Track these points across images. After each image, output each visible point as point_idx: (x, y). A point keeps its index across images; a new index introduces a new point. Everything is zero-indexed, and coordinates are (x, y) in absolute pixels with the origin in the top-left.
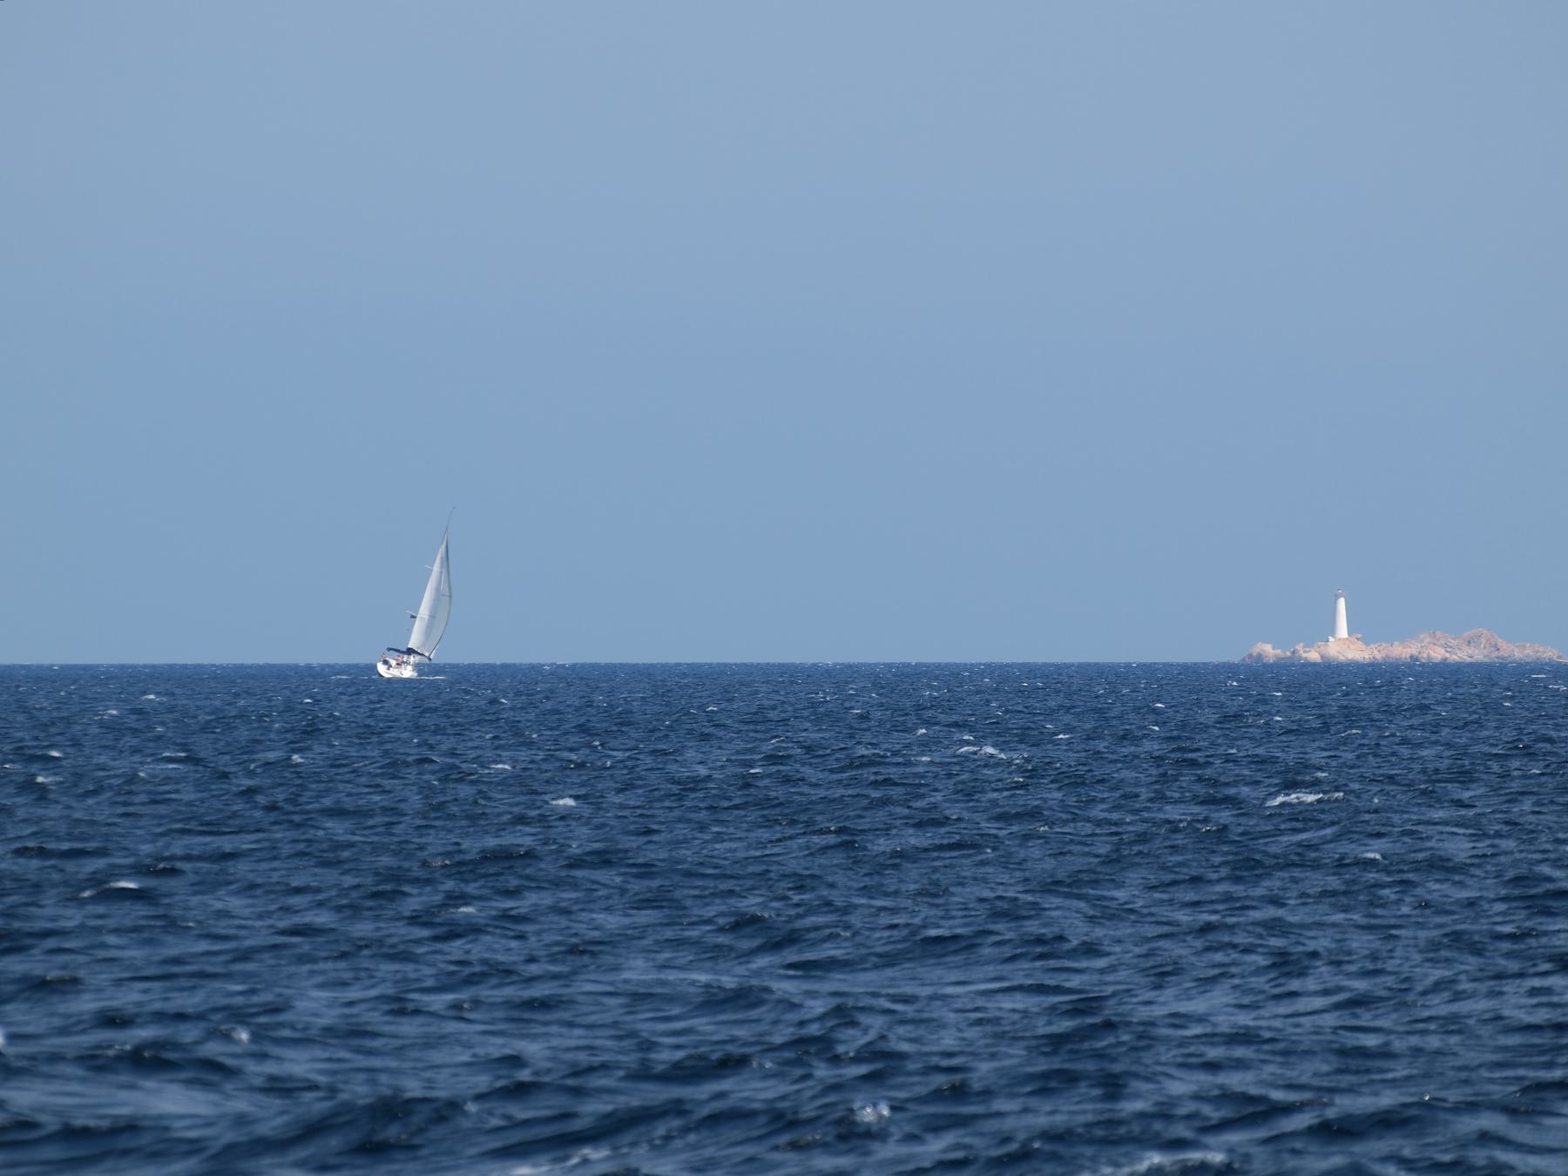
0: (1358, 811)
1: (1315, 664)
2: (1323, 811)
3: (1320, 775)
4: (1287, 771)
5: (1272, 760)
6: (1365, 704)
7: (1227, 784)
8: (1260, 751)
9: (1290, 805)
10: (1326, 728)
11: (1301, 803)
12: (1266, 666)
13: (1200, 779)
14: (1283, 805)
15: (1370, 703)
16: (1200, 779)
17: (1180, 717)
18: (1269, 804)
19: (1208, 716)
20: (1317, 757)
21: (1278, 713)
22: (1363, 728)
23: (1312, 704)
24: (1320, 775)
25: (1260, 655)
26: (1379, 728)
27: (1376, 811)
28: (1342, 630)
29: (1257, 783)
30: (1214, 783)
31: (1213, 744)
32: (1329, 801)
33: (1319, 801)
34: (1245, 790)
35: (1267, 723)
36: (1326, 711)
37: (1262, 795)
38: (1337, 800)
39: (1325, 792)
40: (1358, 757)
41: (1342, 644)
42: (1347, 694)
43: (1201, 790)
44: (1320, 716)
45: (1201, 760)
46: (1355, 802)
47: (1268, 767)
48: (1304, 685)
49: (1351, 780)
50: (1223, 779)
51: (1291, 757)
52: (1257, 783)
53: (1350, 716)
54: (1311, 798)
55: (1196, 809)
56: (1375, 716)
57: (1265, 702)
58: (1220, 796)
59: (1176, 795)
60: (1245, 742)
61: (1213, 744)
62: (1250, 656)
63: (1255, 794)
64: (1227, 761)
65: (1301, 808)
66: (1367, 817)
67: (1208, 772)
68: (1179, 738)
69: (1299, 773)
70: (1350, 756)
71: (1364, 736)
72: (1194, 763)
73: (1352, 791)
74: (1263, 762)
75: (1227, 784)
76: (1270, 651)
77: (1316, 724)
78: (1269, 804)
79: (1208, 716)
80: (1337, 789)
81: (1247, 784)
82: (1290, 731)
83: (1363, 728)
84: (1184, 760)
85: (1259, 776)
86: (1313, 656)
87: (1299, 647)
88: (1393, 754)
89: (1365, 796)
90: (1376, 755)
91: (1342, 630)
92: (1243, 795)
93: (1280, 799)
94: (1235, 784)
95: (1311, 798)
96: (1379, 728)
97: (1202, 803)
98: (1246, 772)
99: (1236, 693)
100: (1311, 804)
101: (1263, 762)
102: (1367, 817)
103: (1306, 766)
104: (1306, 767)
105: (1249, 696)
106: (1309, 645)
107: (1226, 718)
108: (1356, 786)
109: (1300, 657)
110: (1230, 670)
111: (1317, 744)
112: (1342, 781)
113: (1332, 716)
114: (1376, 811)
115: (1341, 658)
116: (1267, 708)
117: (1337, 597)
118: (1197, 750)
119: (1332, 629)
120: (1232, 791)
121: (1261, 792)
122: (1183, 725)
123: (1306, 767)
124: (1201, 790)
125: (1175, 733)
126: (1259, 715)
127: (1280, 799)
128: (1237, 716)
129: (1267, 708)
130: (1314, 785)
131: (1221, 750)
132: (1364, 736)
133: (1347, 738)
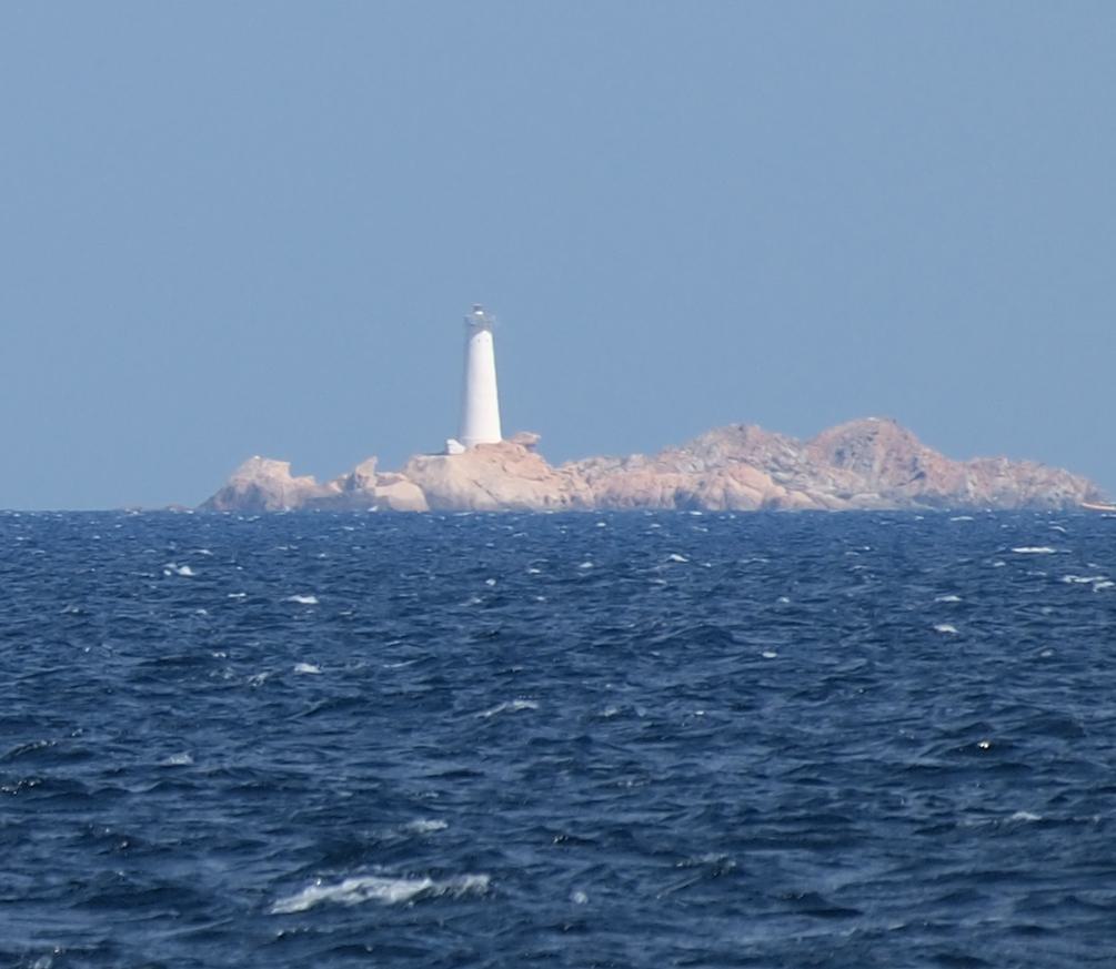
0: (529, 927)
1: (410, 517)
2: (431, 928)
3: (424, 825)
4: (333, 813)
5: (292, 785)
6: (549, 628)
7: (164, 852)
8: (257, 759)
9: (339, 909)
10: (439, 695)
11: (369, 905)
12: (272, 521)
13: (88, 838)
14: (321, 909)
15: (562, 625)
16: (88, 838)
17: (32, 664)
18: (282, 905)
19: (112, 662)
20: (414, 776)
21: (307, 652)
22: (544, 694)
23: (402, 627)
24: (424, 825)
25: (255, 491)
26: (590, 695)
27: (580, 927)
28: (486, 421)
29: (248, 847)
30: (128, 847)
31: (125, 740)
32: (448, 898)
33: (422, 899)
34: (215, 868)
35: (275, 682)
36: (440, 647)
37: (262, 882)
38: (470, 896)
39: (437, 874)
40: (530, 776)
41: (490, 460)
42: (499, 600)
43: (92, 868)
44: (423, 662)
45: (93, 785)
46: (520, 899)
47: (279, 803)
48: (379, 574)
49: (510, 841)
50: (152, 837)
51: (342, 776)
52: (248, 847)
53: (507, 660)
54: (398, 891)
55: (78, 921)
56: (579, 661)
57: (271, 623)
58: (143, 883)
59: (23, 882)
60: (213, 734)
61: (125, 740)
62: (229, 494)
63: (242, 879)
64: (164, 787)
65: (371, 917)
66: (554, 943)
67: (112, 818)
68: (29, 722)
69: (364, 821)
70: (507, 772)
71: (546, 718)
72: (71, 793)
73: (514, 872)
74: (266, 789)
75: (164, 852)
76: (282, 480)
77: (412, 684)
78: (282, 905)
79: (112, 662)
80: (471, 866)
81: (218, 851)
82: (342, 704)
83: (544, 694)
84: (45, 785)
85: (253, 829)
86: (405, 493)
87: (367, 470)
88: (628, 767)
89: (549, 885)
90: (579, 771)
91: (486, 421)
92: (209, 883)
93: (312, 893)
94: (187, 850)
95: (398, 891)
96: (590, 695)
97: (97, 903)
98: (217, 818)
99: (190, 596)
100: (399, 906)
101: (266, 789)
102: (554, 943)
103: (383, 801)
104: (385, 804)
105: (225, 606)
106: (394, 462)
107: (161, 667)
108: (523, 857)
109: (369, 498)
110: (174, 532)
111: (414, 740)
112: (484, 843)
113: (459, 661)
114: (580, 927)
115: (483, 500)
116: (277, 638)
117: (472, 329)
118: (81, 756)
119: (458, 424)
120: (177, 871)
121: (259, 873)
122: (42, 687)
123: (385, 804)
124: (92, 868)
125: (19, 709)
126: (254, 657)
127: (312, 893)
128: (193, 662)
129: (277, 638)
130: (408, 854)
131: (147, 757)
132: (546, 718)
133: (498, 722)
